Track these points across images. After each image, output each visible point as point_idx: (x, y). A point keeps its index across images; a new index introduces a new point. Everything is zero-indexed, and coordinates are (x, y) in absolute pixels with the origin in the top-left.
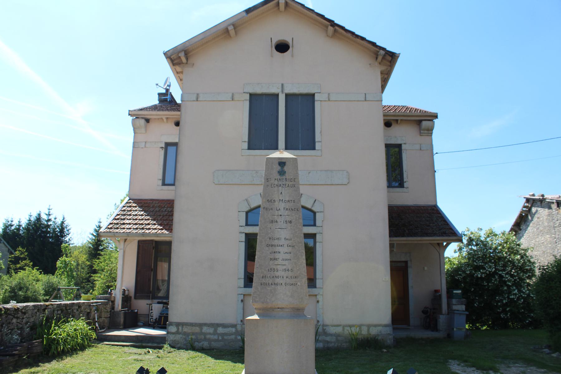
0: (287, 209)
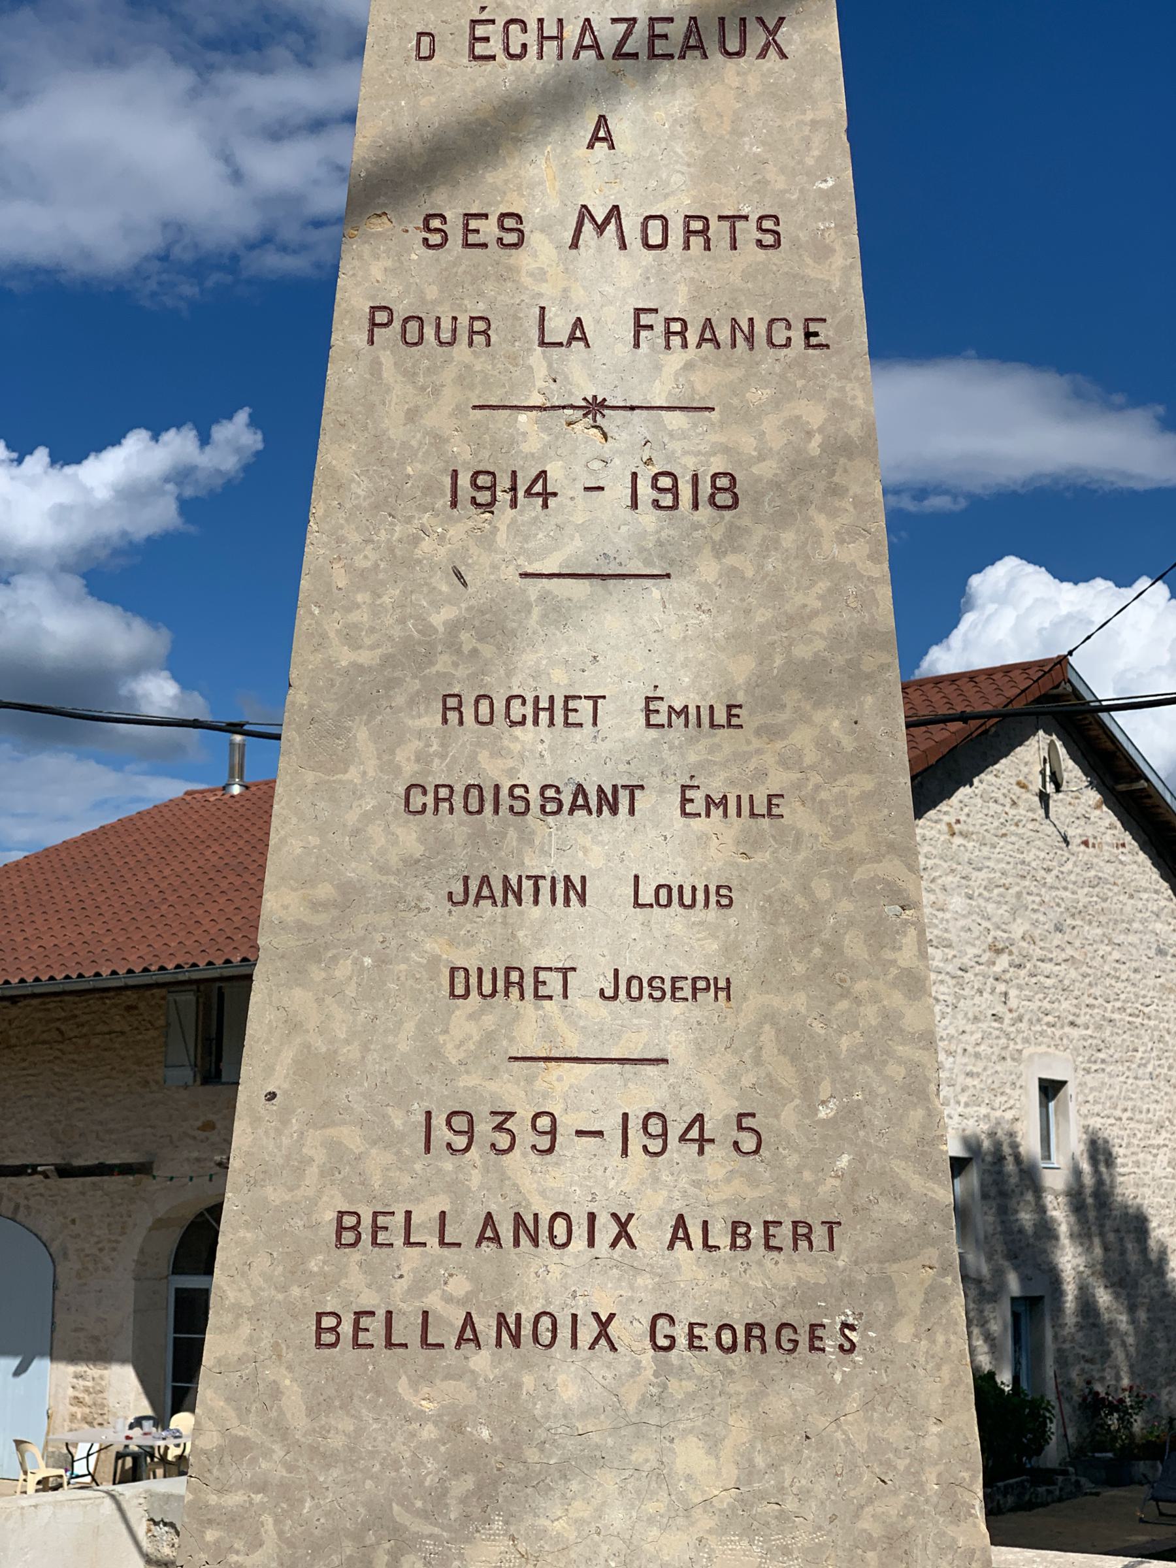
0: (676, 329)
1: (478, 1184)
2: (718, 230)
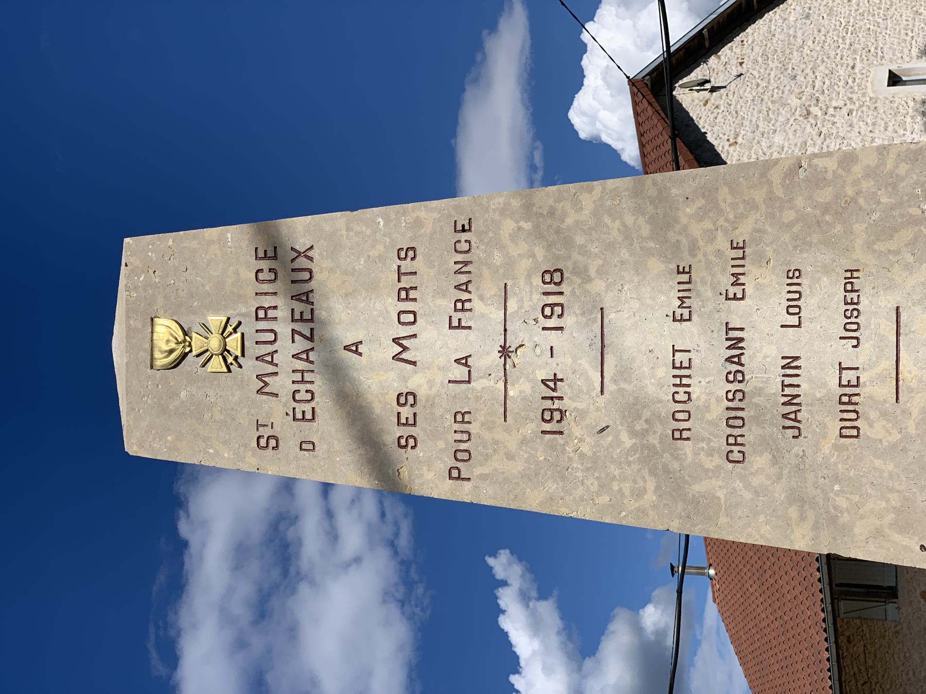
0: (461, 306)
2: (406, 282)
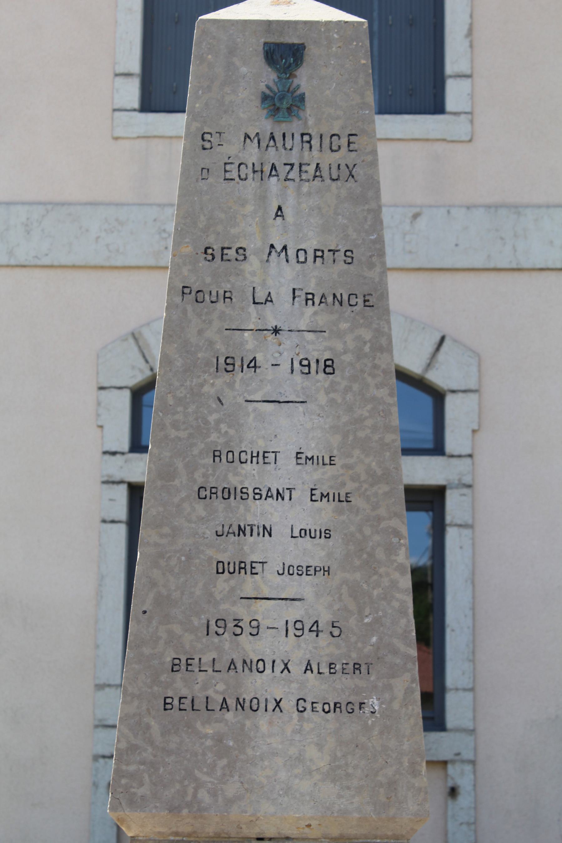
0: (309, 298)
1: (227, 647)
